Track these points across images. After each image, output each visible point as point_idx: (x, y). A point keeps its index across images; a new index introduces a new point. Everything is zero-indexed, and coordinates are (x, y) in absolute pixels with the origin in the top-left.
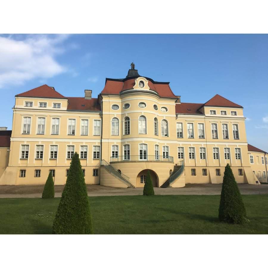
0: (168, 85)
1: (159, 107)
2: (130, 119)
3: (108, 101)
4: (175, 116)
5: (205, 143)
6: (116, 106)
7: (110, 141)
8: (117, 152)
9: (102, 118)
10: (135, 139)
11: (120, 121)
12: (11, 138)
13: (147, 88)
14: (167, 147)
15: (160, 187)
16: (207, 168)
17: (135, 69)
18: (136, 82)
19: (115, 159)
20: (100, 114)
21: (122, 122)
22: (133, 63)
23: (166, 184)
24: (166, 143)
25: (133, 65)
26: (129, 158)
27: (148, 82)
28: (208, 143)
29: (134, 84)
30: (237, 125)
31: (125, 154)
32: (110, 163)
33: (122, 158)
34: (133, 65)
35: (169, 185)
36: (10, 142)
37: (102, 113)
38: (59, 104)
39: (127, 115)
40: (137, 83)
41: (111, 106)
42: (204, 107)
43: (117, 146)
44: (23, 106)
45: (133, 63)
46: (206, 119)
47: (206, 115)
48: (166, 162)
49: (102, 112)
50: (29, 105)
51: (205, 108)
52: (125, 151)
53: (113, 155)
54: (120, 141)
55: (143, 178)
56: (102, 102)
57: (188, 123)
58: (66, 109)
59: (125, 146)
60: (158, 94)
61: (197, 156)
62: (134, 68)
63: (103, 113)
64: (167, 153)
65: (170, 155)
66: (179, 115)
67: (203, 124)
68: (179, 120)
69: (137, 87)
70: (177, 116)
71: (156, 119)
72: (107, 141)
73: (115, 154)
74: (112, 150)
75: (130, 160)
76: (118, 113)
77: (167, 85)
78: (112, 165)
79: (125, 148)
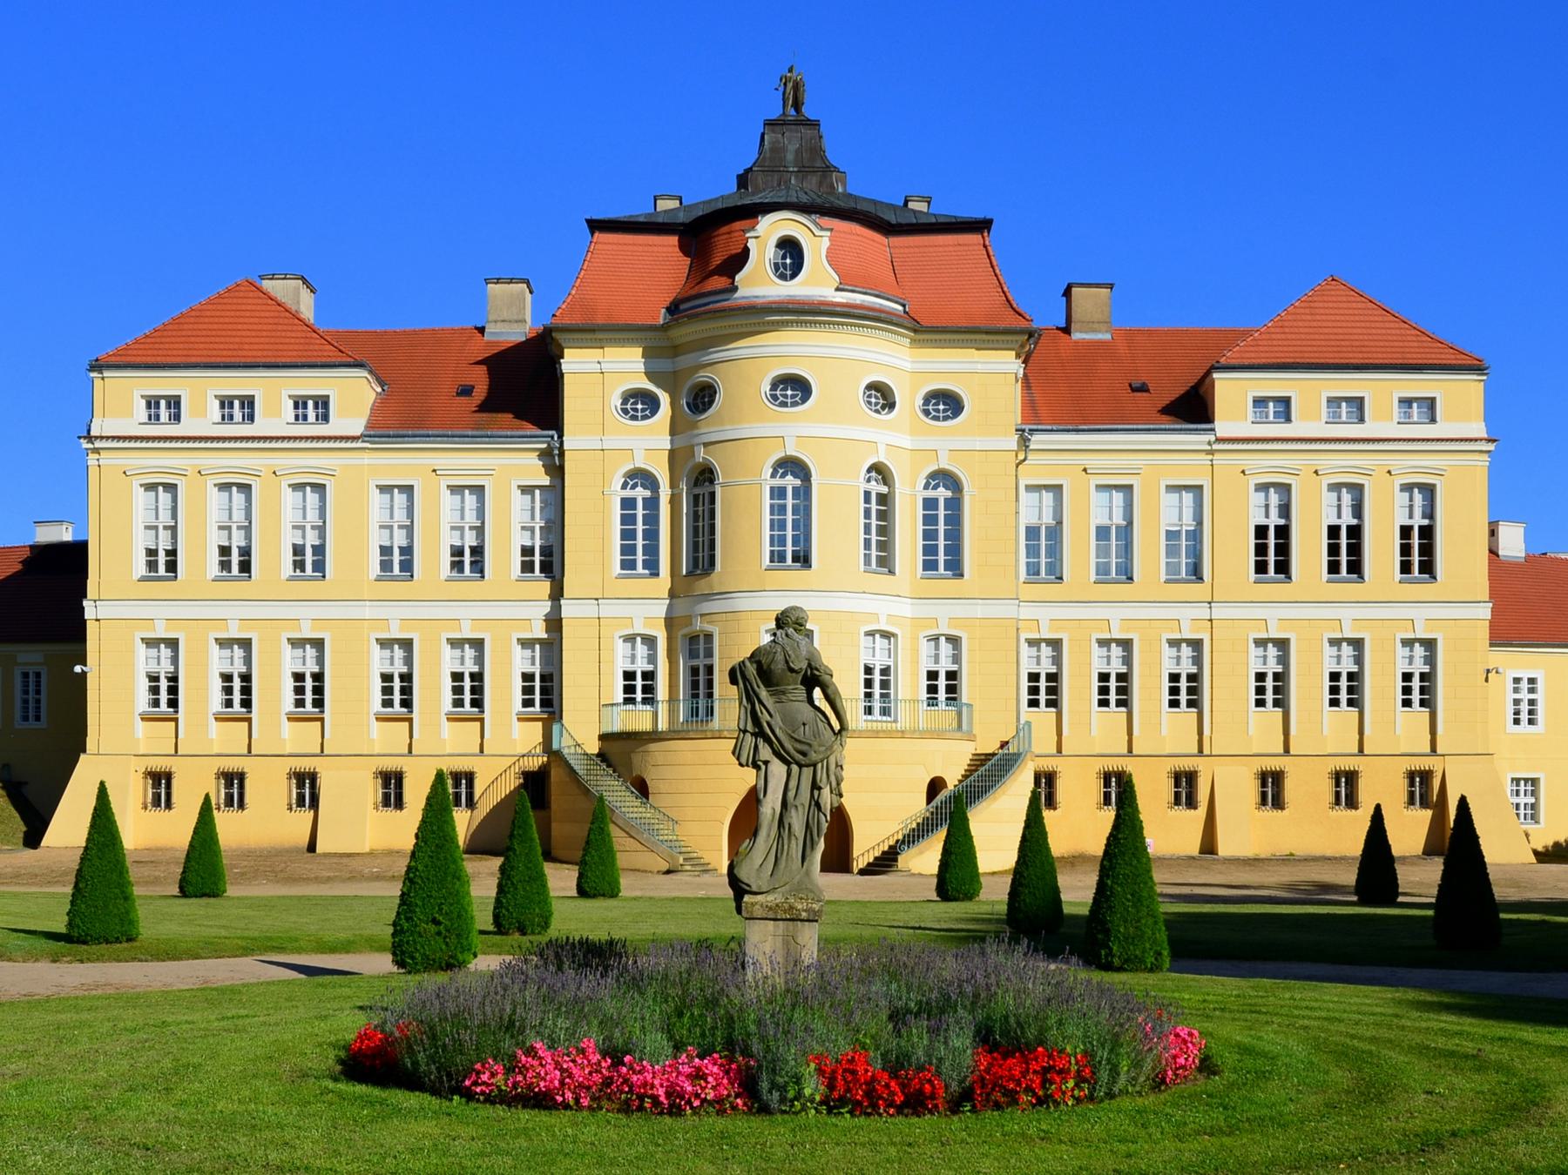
1: (909, 398)
4: (1012, 442)
5: (1203, 612)
6: (639, 403)
7: (608, 609)
8: (649, 676)
12: (85, 603)
14: (954, 641)
15: (855, 870)
16: (1203, 767)
17: (808, 111)
20: (545, 455)
23: (885, 862)
24: (945, 616)
26: (710, 712)
28: (1219, 612)
30: (1429, 491)
32: (604, 737)
33: (672, 713)
35: (896, 860)
36: (84, 622)
37: (562, 443)
38: (323, 403)
39: (701, 454)
40: (762, 253)
41: (617, 402)
42: (1215, 375)
43: (650, 641)
44: (134, 420)
46: (1217, 456)
47: (1223, 426)
48: (875, 734)
49: (561, 436)
50: (164, 413)
51: (1218, 385)
53: (629, 689)
54: (660, 609)
56: (562, 374)
57: (1100, 488)
58: (356, 425)
60: (904, 306)
61: (1149, 689)
62: (797, 105)
63: (566, 447)
64: (951, 675)
65: (965, 694)
66: (1036, 438)
67: (1197, 490)
68: (1039, 469)
70: (1024, 442)
71: (879, 471)
72: (590, 609)
73: (638, 687)
74: (621, 665)
77: (974, 239)
79: (693, 654)
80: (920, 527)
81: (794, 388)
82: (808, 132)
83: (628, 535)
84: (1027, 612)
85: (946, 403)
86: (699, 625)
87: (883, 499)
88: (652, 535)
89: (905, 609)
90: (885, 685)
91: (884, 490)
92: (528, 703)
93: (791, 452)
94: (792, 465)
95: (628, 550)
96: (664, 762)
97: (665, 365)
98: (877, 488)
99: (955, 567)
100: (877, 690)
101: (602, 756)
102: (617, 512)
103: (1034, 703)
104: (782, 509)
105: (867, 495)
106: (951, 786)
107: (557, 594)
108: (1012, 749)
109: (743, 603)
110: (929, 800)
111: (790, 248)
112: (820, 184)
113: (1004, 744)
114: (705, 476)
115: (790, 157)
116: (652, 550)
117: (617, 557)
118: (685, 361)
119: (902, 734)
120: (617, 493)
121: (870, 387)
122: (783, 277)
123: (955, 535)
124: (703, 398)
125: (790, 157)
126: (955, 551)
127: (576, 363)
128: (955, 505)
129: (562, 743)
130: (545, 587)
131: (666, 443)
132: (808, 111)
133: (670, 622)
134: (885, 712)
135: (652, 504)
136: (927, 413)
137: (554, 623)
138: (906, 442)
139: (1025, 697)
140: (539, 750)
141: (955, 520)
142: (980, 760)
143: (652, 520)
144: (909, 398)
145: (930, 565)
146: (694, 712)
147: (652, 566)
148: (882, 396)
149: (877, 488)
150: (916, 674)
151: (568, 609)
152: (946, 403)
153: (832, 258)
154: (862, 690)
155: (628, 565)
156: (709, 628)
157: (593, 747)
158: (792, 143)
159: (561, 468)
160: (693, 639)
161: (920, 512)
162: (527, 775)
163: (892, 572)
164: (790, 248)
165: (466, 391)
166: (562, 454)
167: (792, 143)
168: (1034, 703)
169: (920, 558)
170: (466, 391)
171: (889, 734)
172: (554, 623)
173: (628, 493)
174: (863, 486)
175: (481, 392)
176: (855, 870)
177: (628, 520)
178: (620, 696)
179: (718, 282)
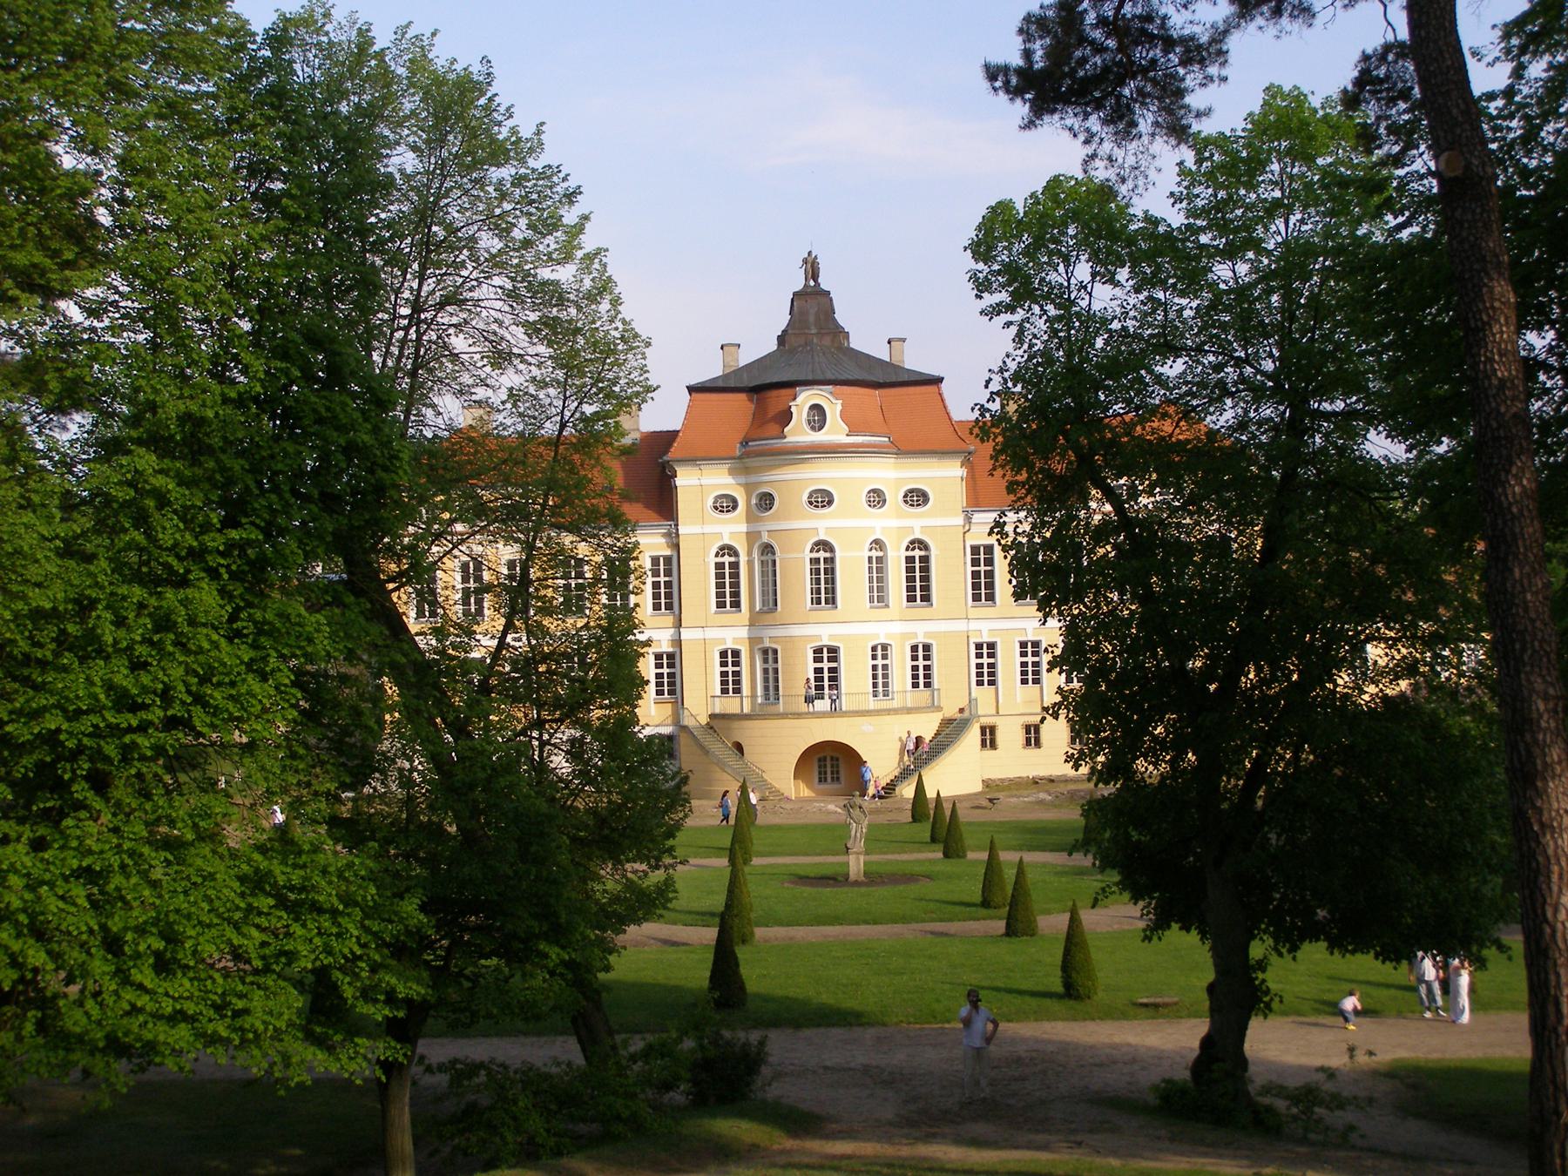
0: (939, 389)
2: (778, 553)
3: (697, 482)
4: (960, 520)
6: (726, 504)
7: (711, 633)
9: (677, 547)
10: (796, 631)
11: (743, 559)
13: (835, 432)
18: (793, 409)
19: (731, 705)
20: (668, 535)
21: (750, 563)
22: (810, 253)
23: (890, 788)
24: (921, 631)
25: (812, 268)
27: (839, 407)
29: (786, 417)
31: (766, 680)
32: (713, 716)
34: (812, 268)
39: (765, 538)
40: (800, 414)
41: (710, 502)
43: (736, 653)
45: (810, 253)
48: (878, 712)
49: (677, 525)
52: (766, 671)
54: (743, 633)
55: (829, 766)
59: (765, 652)
62: (815, 276)
69: (799, 432)
70: (968, 520)
75: (781, 708)
76: (732, 529)
77: (931, 389)
79: (765, 661)
80: (904, 574)
81: (822, 499)
82: (821, 299)
83: (720, 585)
84: (974, 625)
85: (917, 497)
86: (767, 644)
87: (879, 560)
88: (735, 585)
89: (898, 628)
90: (885, 676)
91: (880, 554)
93: (822, 537)
95: (720, 595)
97: (742, 480)
98: (875, 554)
99: (926, 598)
100: (880, 680)
101: (710, 727)
102: (713, 571)
103: (980, 683)
104: (818, 572)
105: (870, 559)
106: (927, 741)
107: (678, 624)
108: (966, 714)
109: (796, 631)
111: (817, 409)
112: (833, 341)
113: (961, 710)
114: (768, 549)
115: (812, 319)
116: (736, 594)
117: (714, 600)
118: (753, 478)
119: (895, 711)
121: (874, 491)
122: (813, 428)
123: (926, 579)
124: (766, 501)
125: (812, 319)
126: (926, 588)
127: (687, 480)
128: (925, 560)
129: (687, 721)
130: (669, 620)
132: (825, 283)
133: (753, 641)
134: (886, 694)
136: (906, 502)
137: (678, 642)
138: (895, 523)
139: (974, 679)
140: (669, 721)
141: (925, 569)
142: (947, 722)
143: (735, 575)
144: (894, 497)
145: (911, 599)
146: (766, 696)
147: (736, 604)
148: (877, 498)
149: (875, 554)
150: (904, 668)
151: (686, 634)
152: (917, 497)
153: (843, 416)
154: (871, 681)
155: (721, 605)
156: (774, 646)
157: (704, 720)
158: (812, 307)
160: (765, 652)
161: (904, 565)
163: (887, 606)
164: (817, 409)
166: (678, 535)
167: (812, 307)
168: (980, 683)
169: (905, 594)
171: (889, 712)
173: (720, 560)
178: (718, 693)
179: (773, 428)
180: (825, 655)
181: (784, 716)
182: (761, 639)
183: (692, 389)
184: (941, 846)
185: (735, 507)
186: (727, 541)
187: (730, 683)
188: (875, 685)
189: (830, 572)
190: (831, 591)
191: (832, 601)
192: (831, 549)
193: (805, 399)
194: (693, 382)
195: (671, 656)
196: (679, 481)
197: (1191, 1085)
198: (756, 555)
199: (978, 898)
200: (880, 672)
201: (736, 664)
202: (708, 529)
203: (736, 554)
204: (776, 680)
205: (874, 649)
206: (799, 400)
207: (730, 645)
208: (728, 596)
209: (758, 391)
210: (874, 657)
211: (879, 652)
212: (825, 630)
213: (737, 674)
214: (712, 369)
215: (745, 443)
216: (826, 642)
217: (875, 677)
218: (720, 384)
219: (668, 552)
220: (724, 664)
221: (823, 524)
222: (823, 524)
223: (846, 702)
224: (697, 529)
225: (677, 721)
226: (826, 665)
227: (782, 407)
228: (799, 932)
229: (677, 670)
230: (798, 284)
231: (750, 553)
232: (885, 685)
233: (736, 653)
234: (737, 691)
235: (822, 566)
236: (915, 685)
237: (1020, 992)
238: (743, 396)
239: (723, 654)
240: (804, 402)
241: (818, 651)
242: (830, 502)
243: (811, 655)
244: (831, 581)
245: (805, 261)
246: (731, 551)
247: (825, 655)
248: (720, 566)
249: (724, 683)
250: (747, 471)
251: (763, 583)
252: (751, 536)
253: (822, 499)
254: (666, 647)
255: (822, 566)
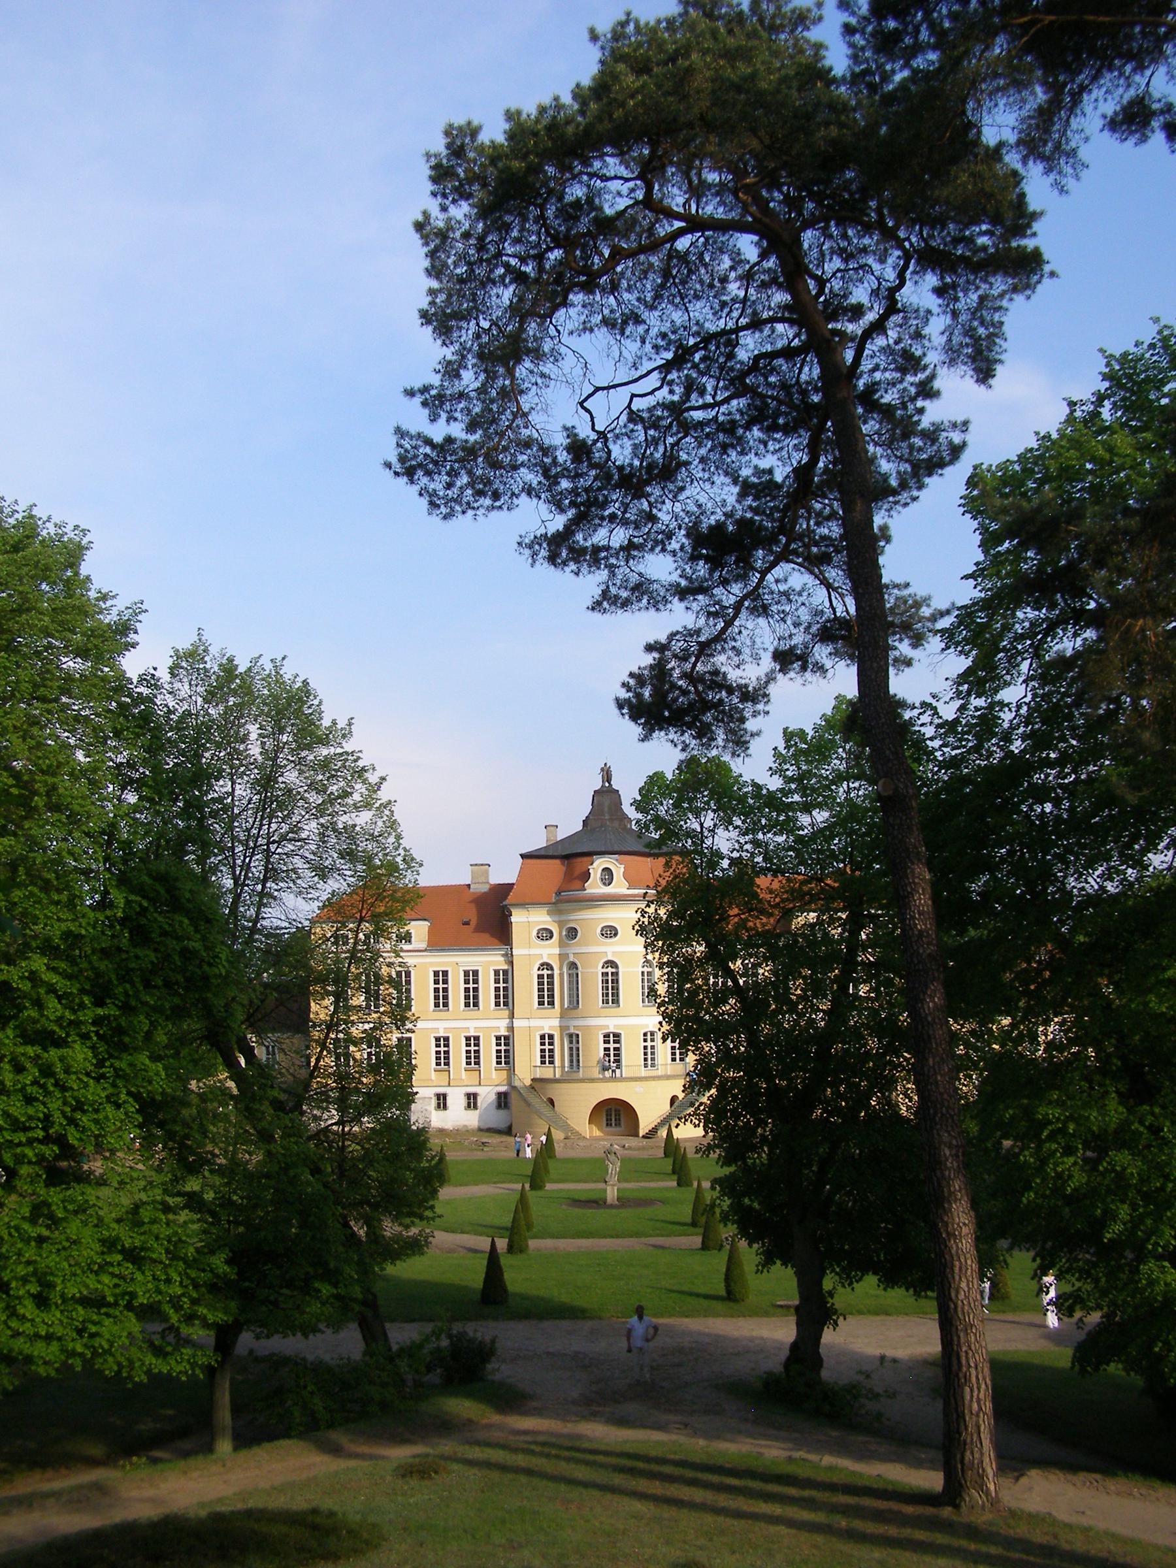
7: (534, 1023)
9: (511, 963)
11: (556, 972)
13: (619, 886)
19: (547, 1072)
21: (561, 975)
23: (653, 1132)
25: (607, 774)
27: (622, 870)
29: (586, 876)
31: (571, 1055)
34: (607, 774)
41: (535, 933)
43: (551, 1037)
52: (571, 1049)
54: (556, 1022)
58: (423, 945)
59: (571, 1036)
62: (609, 781)
69: (595, 886)
75: (581, 1075)
76: (549, 951)
78: (536, 1085)
79: (571, 1042)
81: (610, 932)
83: (540, 990)
86: (572, 1031)
88: (551, 990)
90: (653, 1053)
92: (499, 1063)
93: (610, 958)
94: (611, 963)
95: (541, 997)
96: (561, 1093)
97: (557, 918)
98: (646, 970)
100: (649, 1056)
101: (532, 1087)
107: (512, 1016)
110: (671, 1105)
114: (573, 966)
116: (551, 996)
117: (536, 1000)
118: (564, 918)
120: (536, 973)
122: (604, 884)
124: (572, 933)
125: (606, 809)
127: (518, 918)
129: (517, 1083)
130: (506, 1013)
131: (557, 951)
133: (562, 1028)
134: (653, 1065)
135: (551, 977)
137: (511, 1028)
143: (551, 983)
146: (571, 1066)
147: (551, 1003)
151: (517, 1023)
155: (541, 1003)
157: (528, 1082)
158: (607, 801)
159: (512, 962)
160: (571, 1036)
162: (499, 1095)
164: (607, 871)
165: (467, 923)
167: (607, 801)
170: (467, 923)
171: (654, 1078)
172: (511, 1028)
173: (541, 972)
174: (641, 969)
175: (474, 922)
176: (641, 1133)
177: (540, 983)
178: (539, 1063)
179: (578, 884)
180: (612, 1039)
181: (582, 1080)
182: (568, 1028)
183: (523, 856)
184: (676, 1177)
185: (551, 937)
186: (546, 960)
187: (547, 1057)
188: (646, 1060)
189: (616, 981)
190: (616, 995)
191: (616, 1001)
192: (617, 967)
193: (599, 865)
194: (524, 852)
195: (506, 1038)
196: (513, 919)
197: (784, 1375)
198: (565, 970)
199: (689, 1220)
200: (649, 1051)
201: (551, 1044)
202: (534, 951)
203: (552, 969)
204: (578, 1055)
205: (645, 1034)
206: (595, 865)
207: (547, 1031)
208: (546, 997)
209: (567, 858)
210: (645, 1041)
211: (649, 1037)
212: (611, 1022)
213: (551, 1051)
214: (538, 842)
215: (558, 893)
216: (612, 1029)
217: (645, 1054)
218: (543, 853)
219: (506, 967)
220: (543, 1044)
221: (610, 949)
222: (610, 949)
223: (626, 1072)
224: (525, 952)
225: (510, 1084)
226: (612, 1046)
227: (584, 869)
228: (563, 1244)
229: (510, 1048)
230: (598, 786)
231: (561, 968)
232: (653, 1059)
233: (551, 1037)
234: (552, 1062)
235: (610, 978)
236: (674, 1060)
237: (698, 1295)
238: (558, 861)
239: (542, 1037)
240: (598, 866)
241: (607, 1036)
242: (616, 935)
243: (601, 1039)
244: (616, 989)
245: (602, 770)
246: (549, 967)
247: (612, 1039)
248: (540, 977)
249: (543, 1057)
250: (560, 912)
251: (570, 989)
252: (562, 957)
253: (610, 932)
254: (504, 1032)
255: (610, 978)
